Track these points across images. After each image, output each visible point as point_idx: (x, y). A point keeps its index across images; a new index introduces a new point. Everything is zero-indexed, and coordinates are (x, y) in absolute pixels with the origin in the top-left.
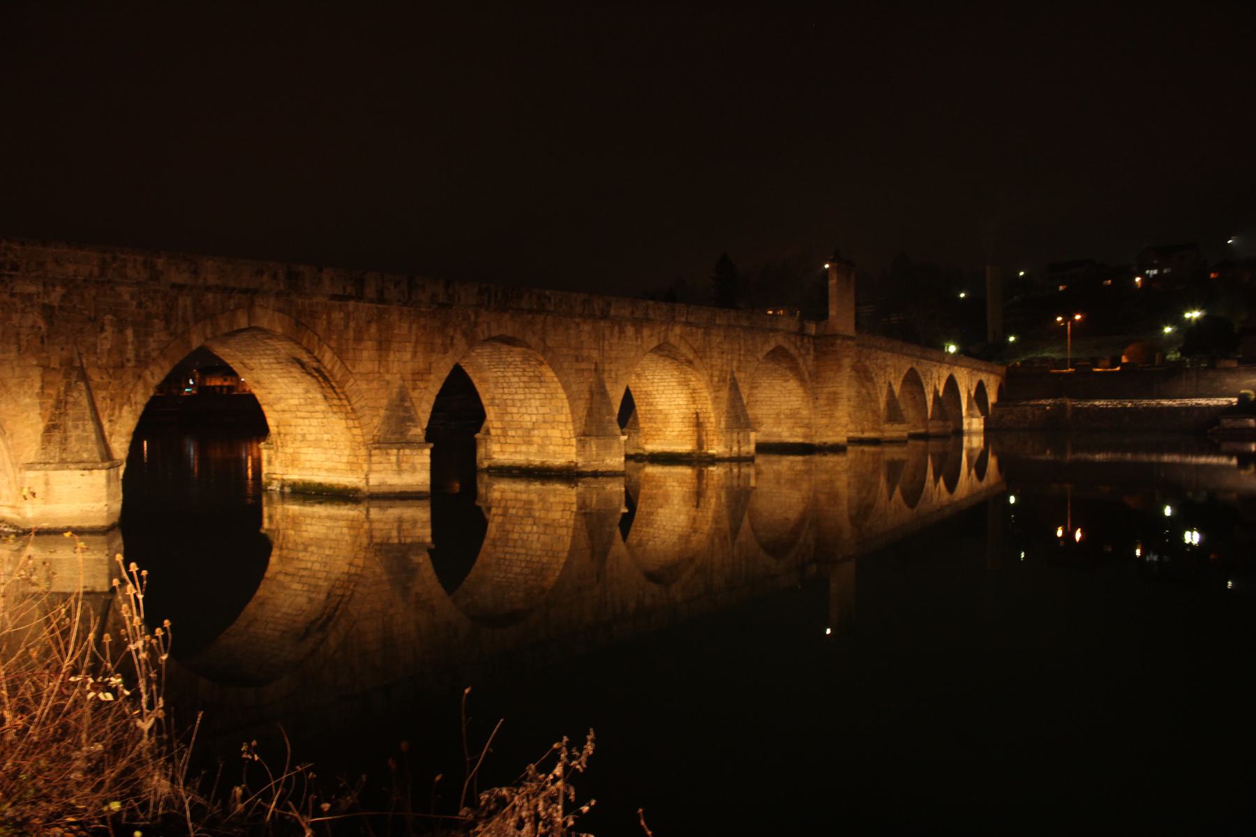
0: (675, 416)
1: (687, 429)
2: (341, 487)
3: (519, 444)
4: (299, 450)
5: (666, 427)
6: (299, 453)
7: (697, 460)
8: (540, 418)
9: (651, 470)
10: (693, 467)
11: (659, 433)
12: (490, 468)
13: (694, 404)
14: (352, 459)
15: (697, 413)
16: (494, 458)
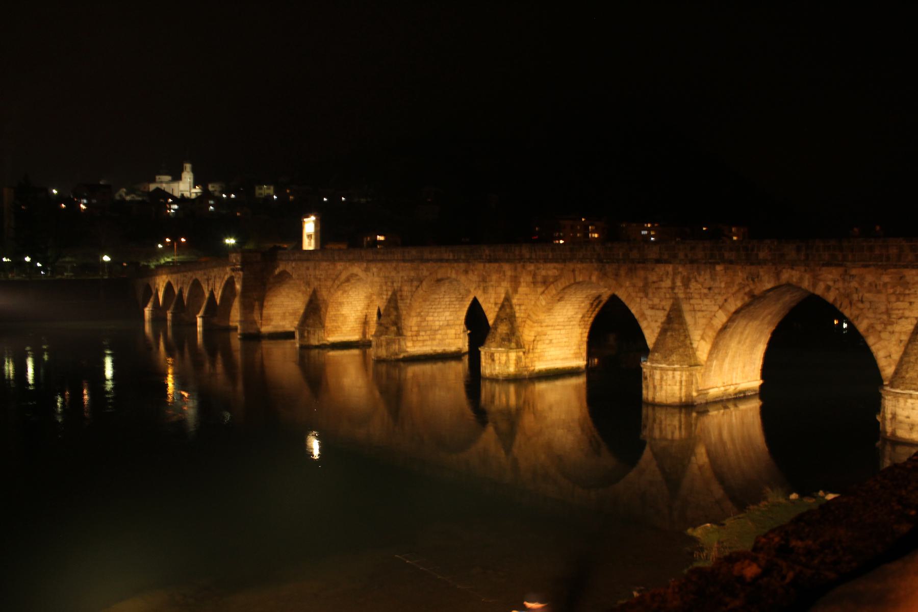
0: (351, 318)
1: (357, 326)
2: (570, 368)
3: (427, 340)
4: (544, 350)
5: (343, 325)
6: (544, 352)
7: (362, 345)
8: (446, 323)
9: (332, 353)
10: (361, 349)
11: (338, 329)
12: (404, 357)
13: (367, 309)
14: (578, 351)
15: (366, 316)
16: (407, 352)
